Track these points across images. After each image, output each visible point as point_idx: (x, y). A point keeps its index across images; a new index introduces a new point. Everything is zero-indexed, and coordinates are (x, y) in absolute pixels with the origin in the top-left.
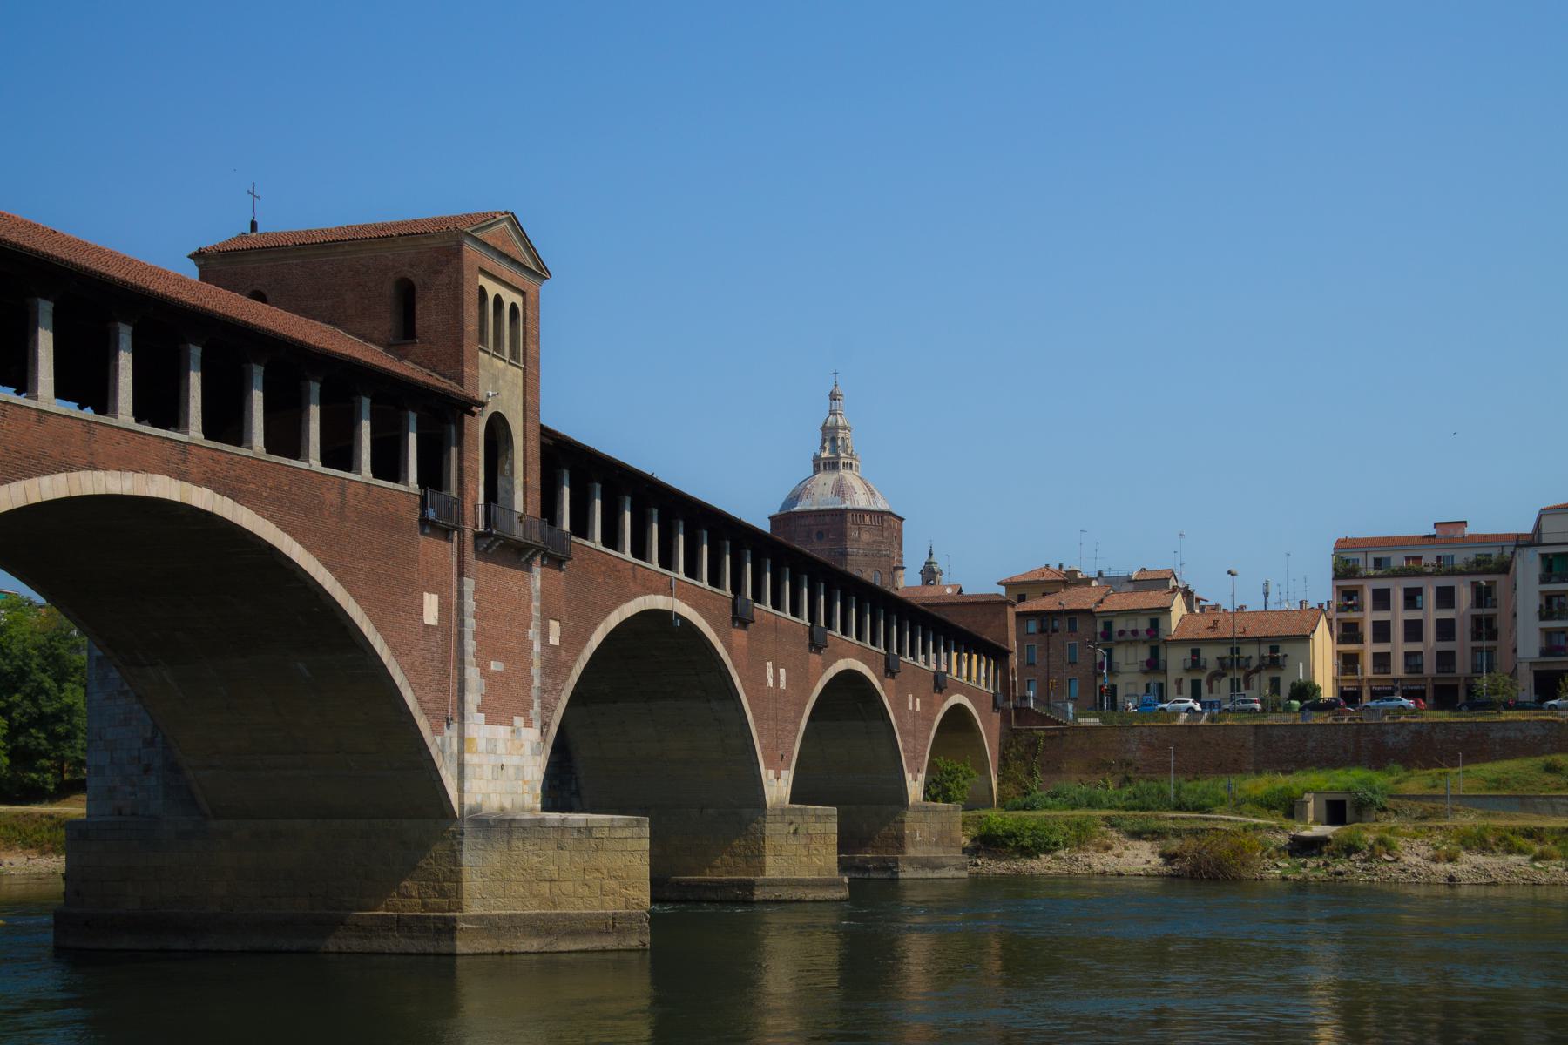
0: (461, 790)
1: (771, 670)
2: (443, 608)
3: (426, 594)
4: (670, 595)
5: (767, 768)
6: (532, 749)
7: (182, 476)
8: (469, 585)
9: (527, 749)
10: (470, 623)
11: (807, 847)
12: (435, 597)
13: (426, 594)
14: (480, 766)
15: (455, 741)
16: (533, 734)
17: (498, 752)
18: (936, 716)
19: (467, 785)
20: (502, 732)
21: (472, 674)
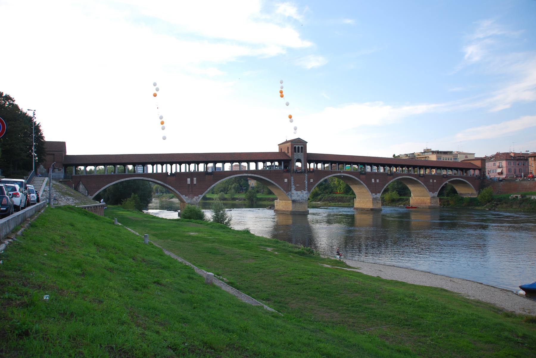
0: (291, 198)
1: (374, 180)
2: (288, 180)
3: (285, 179)
4: (341, 173)
5: (371, 193)
6: (306, 194)
7: (247, 173)
8: (292, 177)
9: (305, 193)
10: (292, 181)
11: (377, 204)
12: (287, 179)
13: (285, 179)
14: (295, 196)
15: (291, 194)
16: (306, 192)
17: (298, 194)
18: (444, 183)
19: (292, 198)
20: (299, 192)
21: (293, 186)
